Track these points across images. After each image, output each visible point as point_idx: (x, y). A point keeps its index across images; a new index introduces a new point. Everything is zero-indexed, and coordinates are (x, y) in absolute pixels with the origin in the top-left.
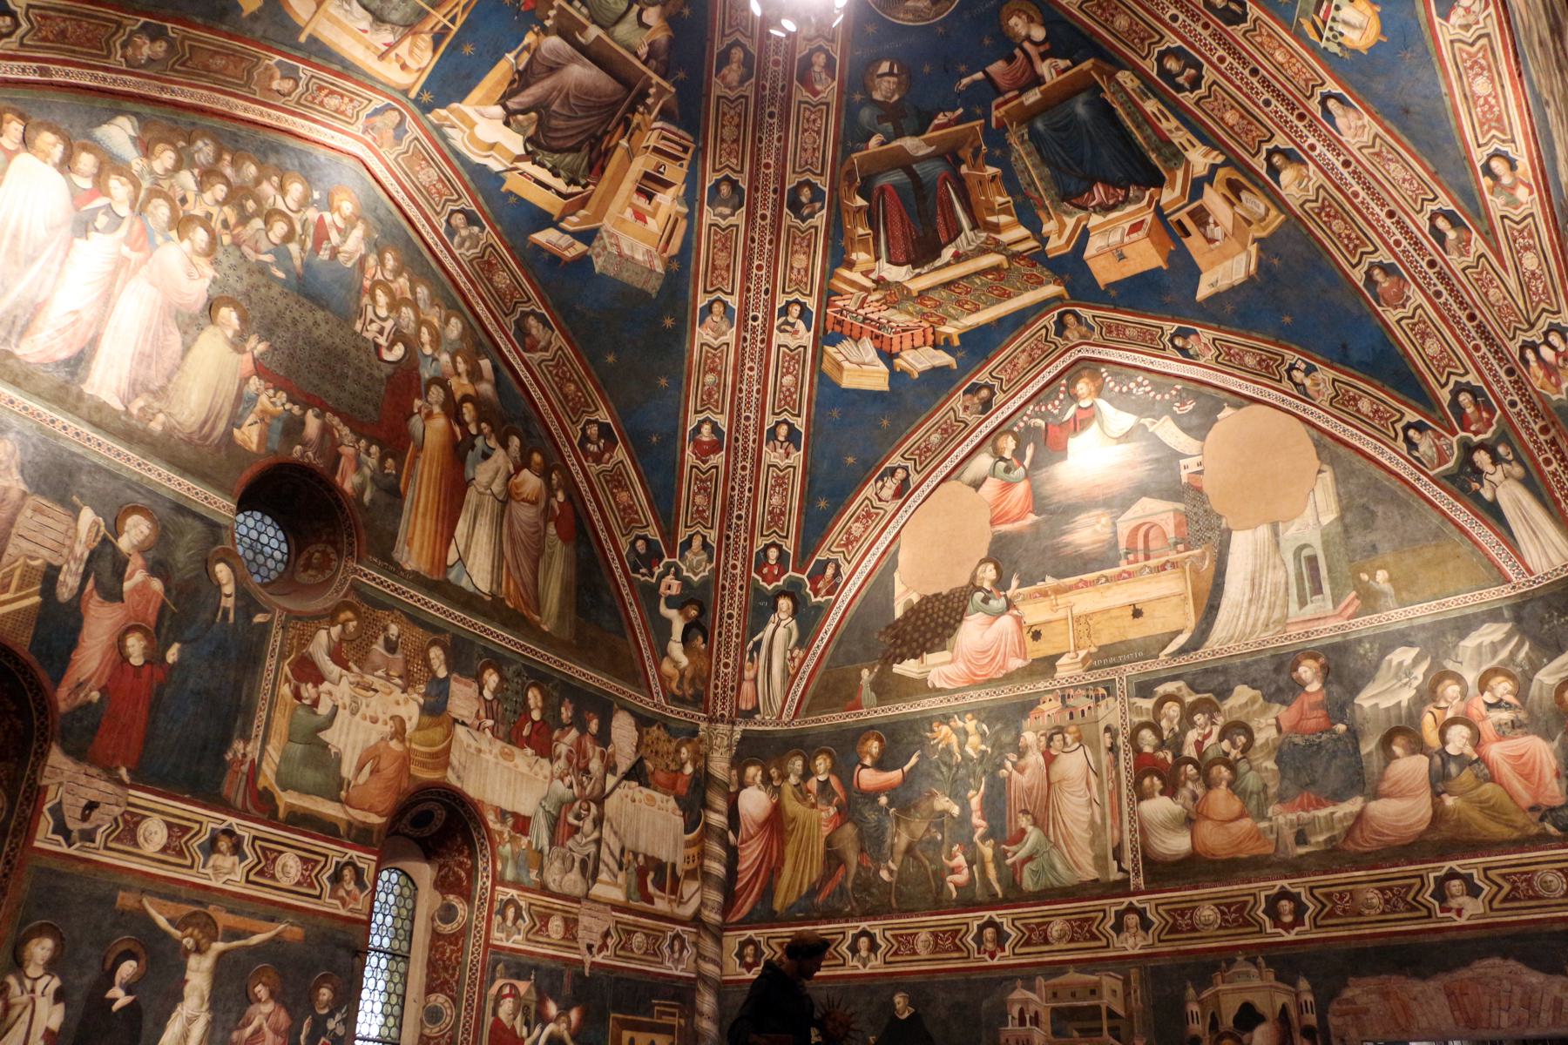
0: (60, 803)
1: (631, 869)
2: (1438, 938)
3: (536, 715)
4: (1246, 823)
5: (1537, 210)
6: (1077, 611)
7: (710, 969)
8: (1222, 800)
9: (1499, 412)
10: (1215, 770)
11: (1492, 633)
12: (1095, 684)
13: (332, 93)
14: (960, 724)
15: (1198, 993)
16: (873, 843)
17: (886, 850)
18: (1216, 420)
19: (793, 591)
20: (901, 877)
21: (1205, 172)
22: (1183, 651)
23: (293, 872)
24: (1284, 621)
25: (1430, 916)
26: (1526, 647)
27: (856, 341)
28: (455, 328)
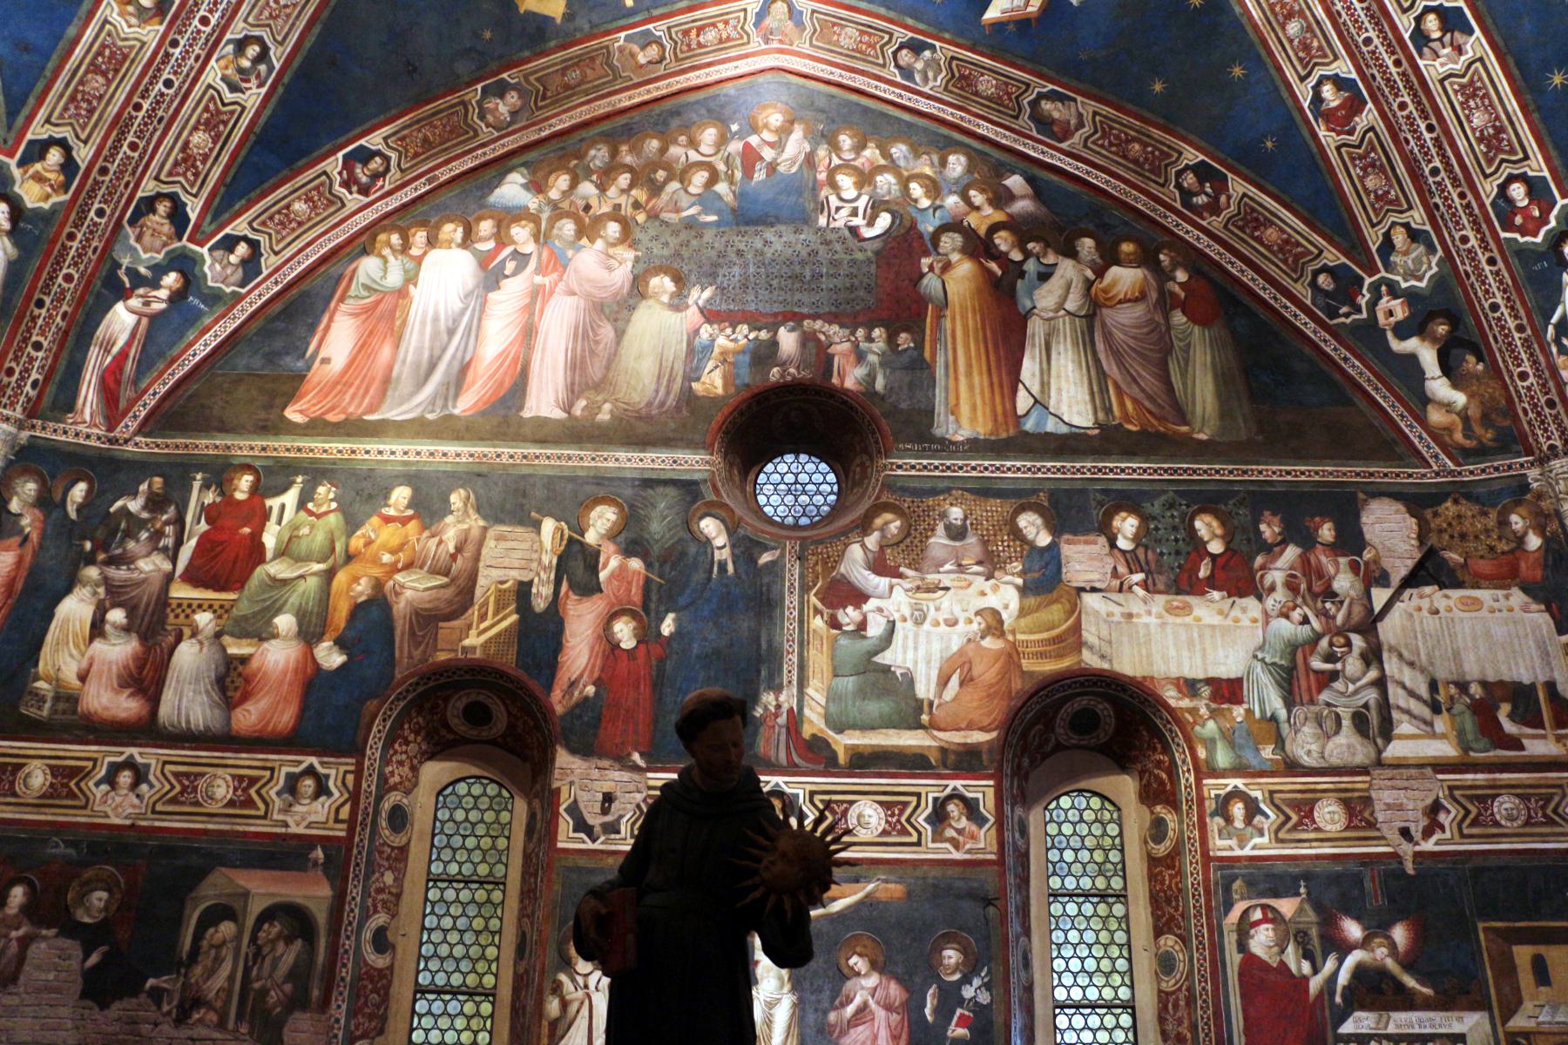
0: (575, 801)
3: (1216, 547)
13: (700, 30)
23: (874, 821)
28: (957, 164)
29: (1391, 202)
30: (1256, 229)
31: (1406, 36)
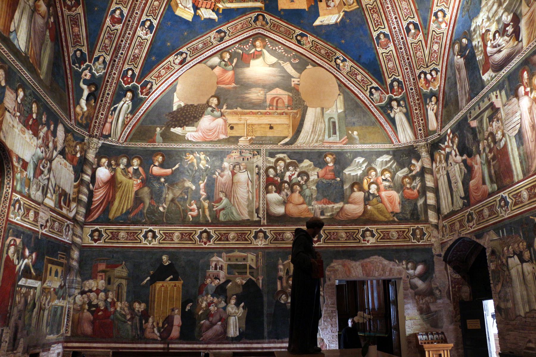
1: (57, 194)
2: (361, 249)
3: (34, 116)
4: (304, 206)
5: (445, 32)
6: (249, 122)
7: (78, 240)
8: (296, 197)
9: (405, 91)
10: (295, 187)
11: (386, 158)
12: (254, 150)
14: (198, 155)
15: (283, 262)
16: (157, 196)
17: (162, 199)
19: (133, 90)
20: (169, 211)
22: (286, 144)
24: (323, 141)
25: (359, 242)
26: (395, 164)
29: (106, 50)
30: (74, 24)
31: (142, 20)
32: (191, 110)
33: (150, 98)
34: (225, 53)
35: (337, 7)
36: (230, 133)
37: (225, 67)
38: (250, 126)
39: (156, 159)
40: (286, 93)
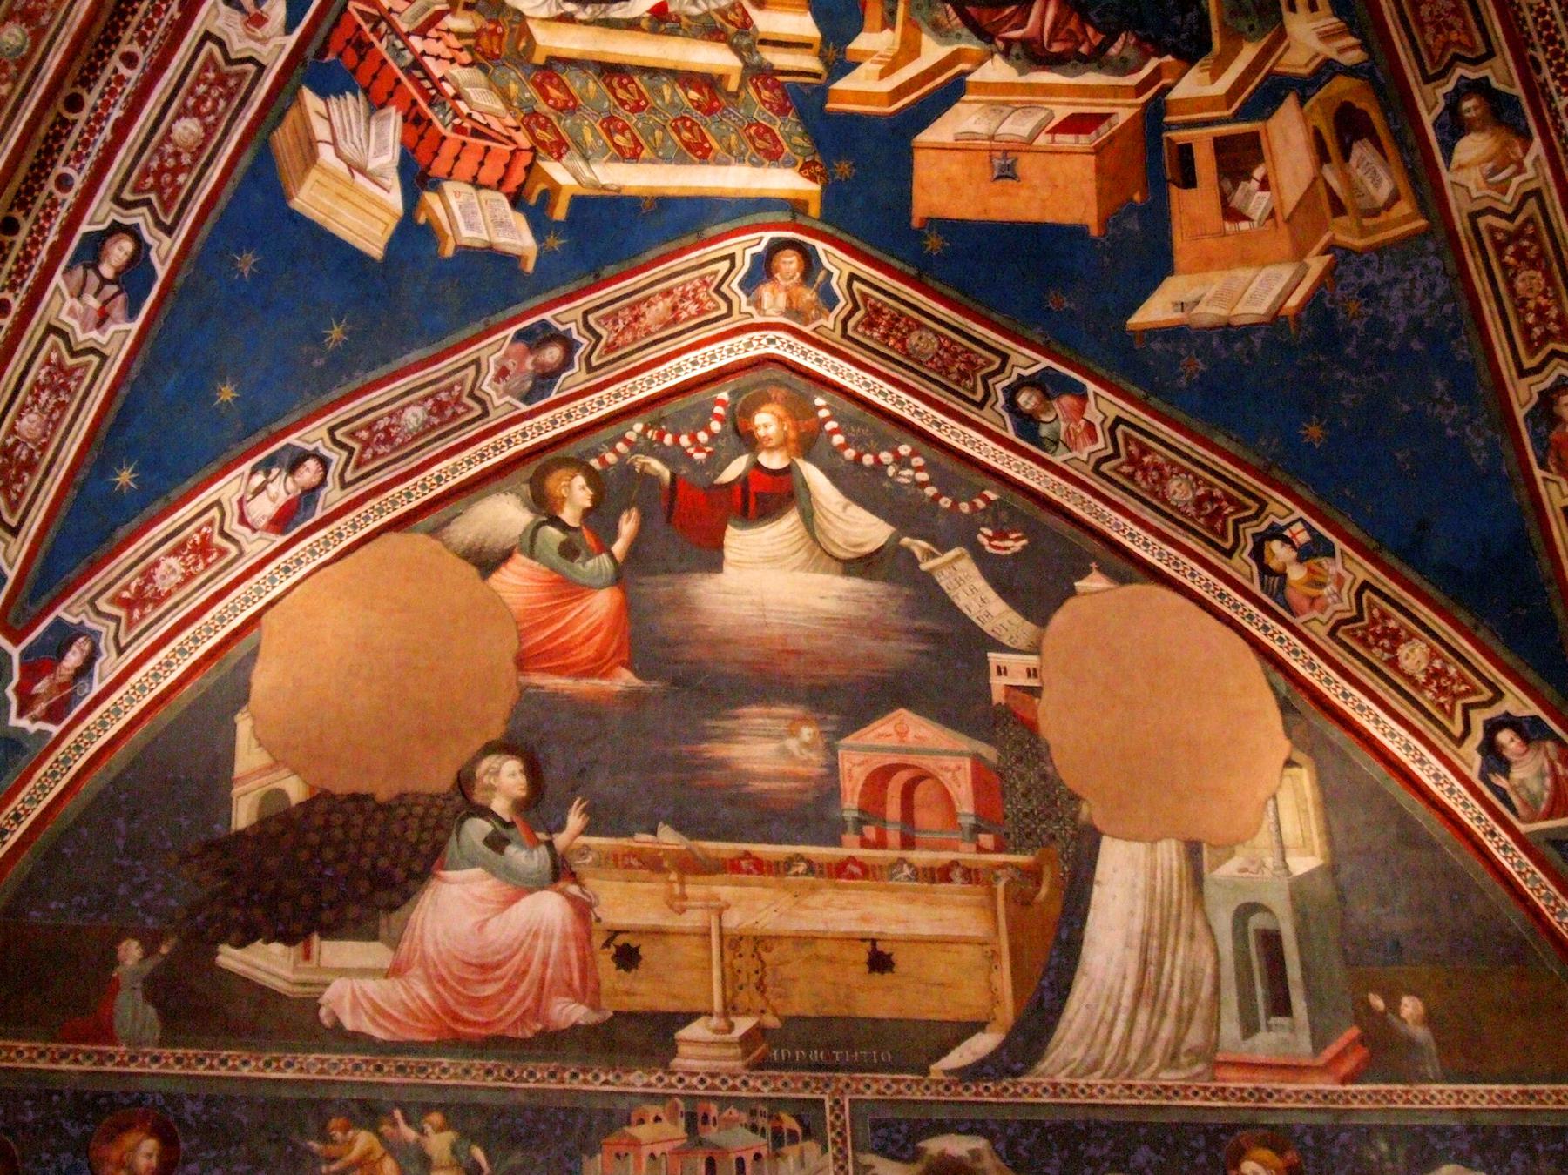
6: (735, 920)
12: (776, 1104)
14: (410, 1134)
18: (1072, 592)
21: (1304, 71)
24: (1210, 1056)
27: (376, 106)
31: (84, 228)
32: (354, 833)
33: (68, 741)
34: (561, 473)
35: (1288, 221)
36: (616, 993)
37: (563, 564)
38: (746, 948)
39: (115, 1154)
40: (965, 743)
